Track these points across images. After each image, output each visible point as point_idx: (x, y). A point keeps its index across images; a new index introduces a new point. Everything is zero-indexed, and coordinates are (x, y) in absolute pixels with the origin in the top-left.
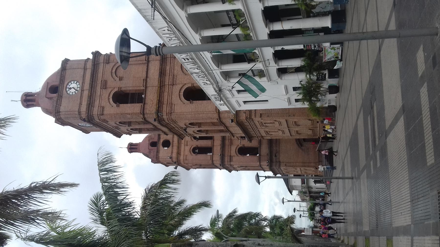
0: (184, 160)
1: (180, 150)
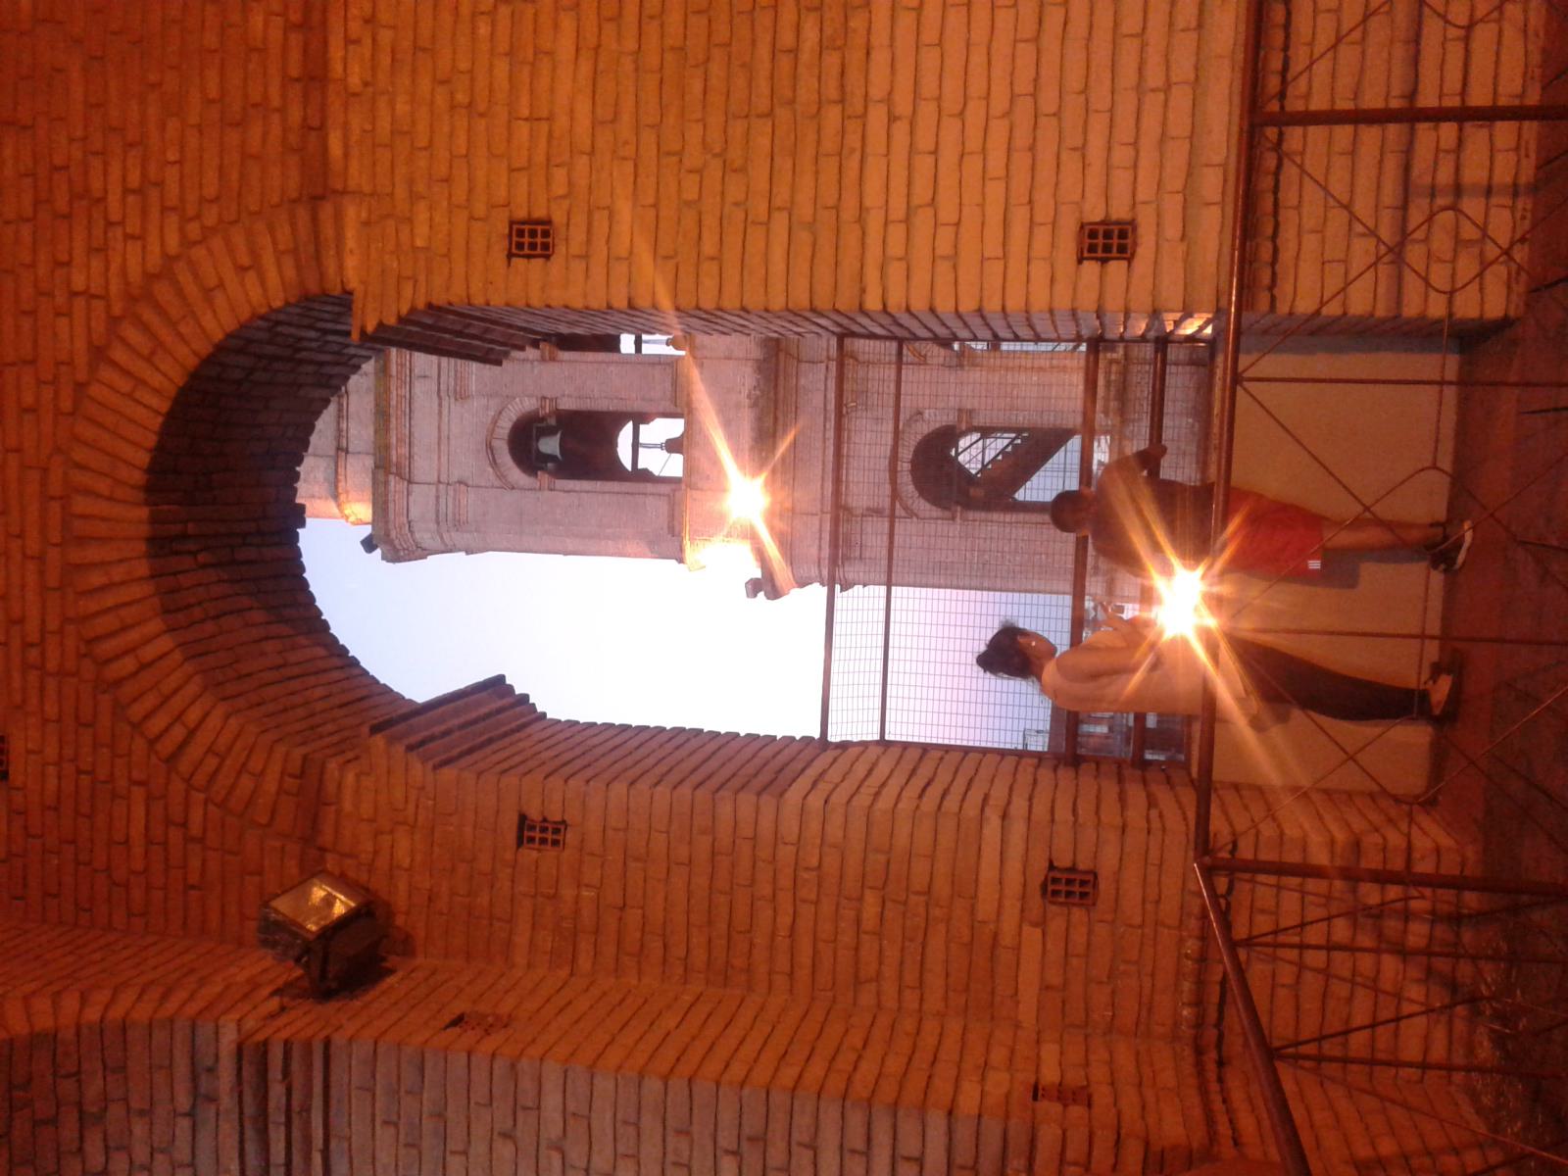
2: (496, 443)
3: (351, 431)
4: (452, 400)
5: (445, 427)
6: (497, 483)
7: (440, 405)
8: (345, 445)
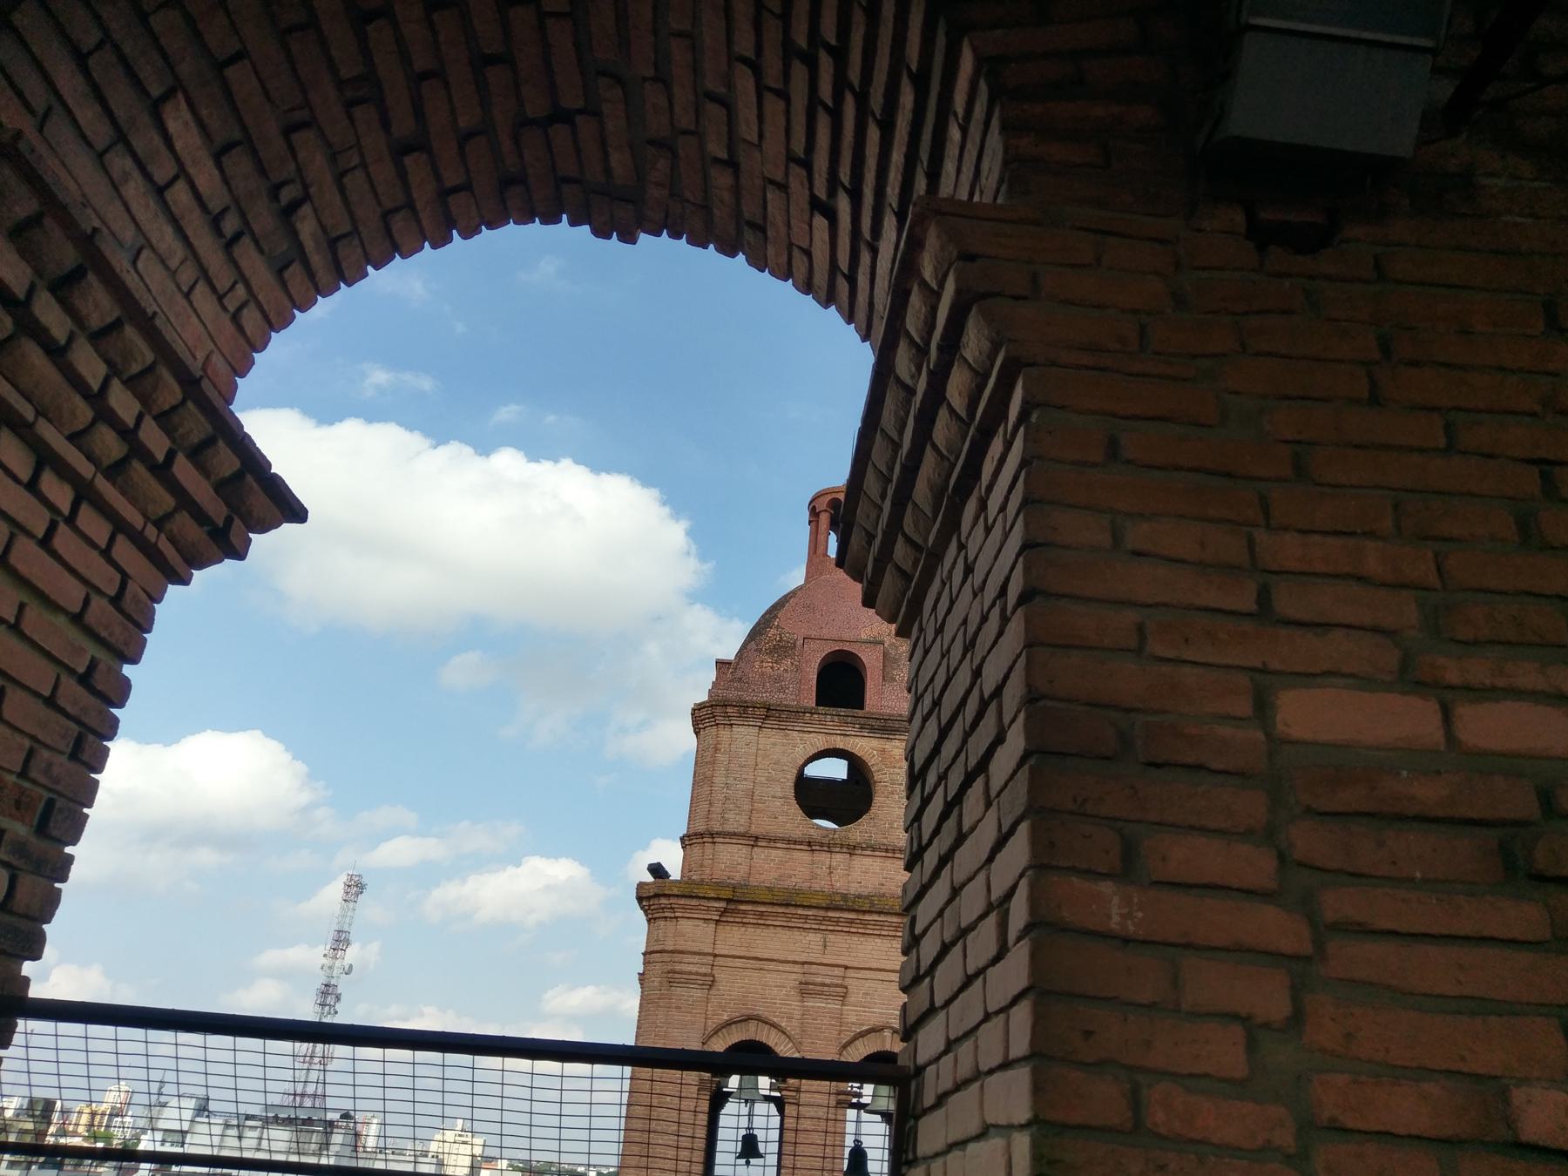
0: (666, 957)
1: (762, 914)
2: (752, 1025)
3: (774, 852)
4: (800, 977)
5: (772, 966)
6: (711, 1025)
7: (795, 962)
8: (760, 844)
